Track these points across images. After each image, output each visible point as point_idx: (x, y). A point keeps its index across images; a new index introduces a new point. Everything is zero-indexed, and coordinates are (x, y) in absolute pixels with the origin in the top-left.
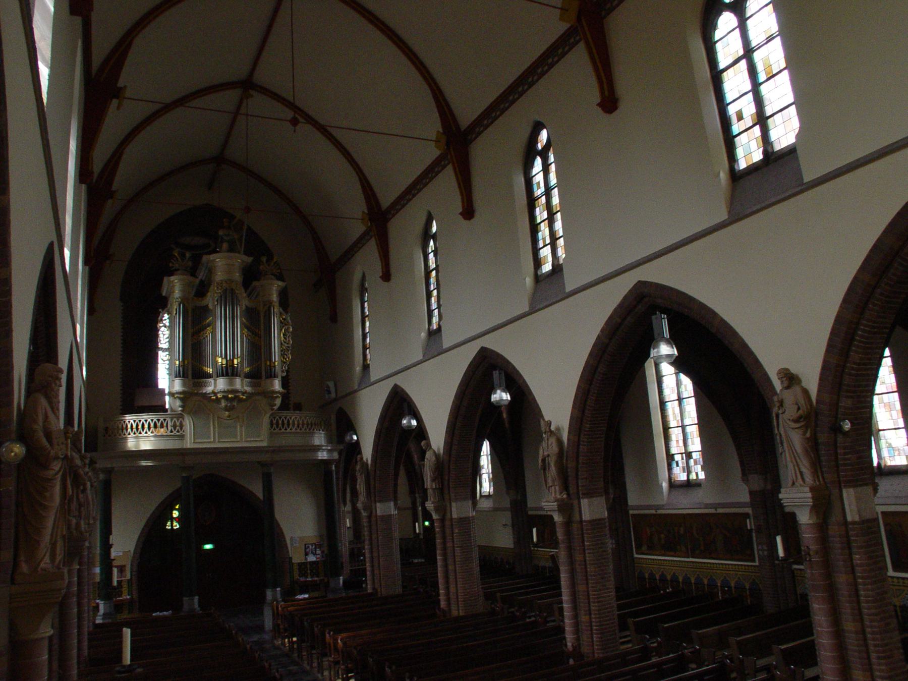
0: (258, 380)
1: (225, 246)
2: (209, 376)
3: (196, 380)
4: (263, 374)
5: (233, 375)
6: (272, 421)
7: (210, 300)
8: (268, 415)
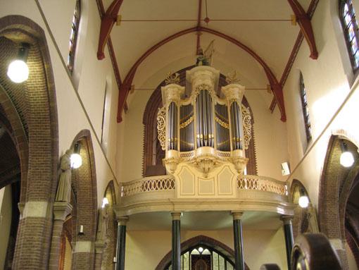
0: (228, 152)
1: (201, 63)
2: (190, 149)
3: (183, 153)
4: (232, 148)
5: (208, 145)
6: (239, 182)
7: (192, 101)
8: (235, 178)
